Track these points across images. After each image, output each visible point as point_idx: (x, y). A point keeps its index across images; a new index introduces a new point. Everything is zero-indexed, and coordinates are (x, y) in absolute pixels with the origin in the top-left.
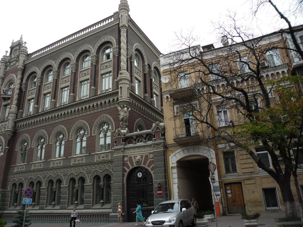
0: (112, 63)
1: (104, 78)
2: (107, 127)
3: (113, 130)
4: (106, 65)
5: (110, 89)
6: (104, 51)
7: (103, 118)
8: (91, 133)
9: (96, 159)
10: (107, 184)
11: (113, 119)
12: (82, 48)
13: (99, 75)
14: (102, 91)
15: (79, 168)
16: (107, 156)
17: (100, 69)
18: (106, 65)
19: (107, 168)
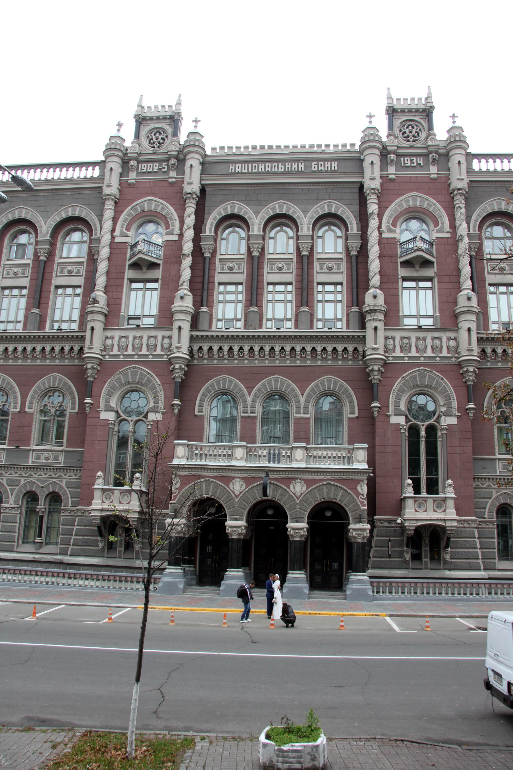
0: (85, 268)
1: (60, 295)
2: (61, 399)
3: (74, 409)
4: (70, 268)
5: (75, 321)
6: (68, 234)
7: (54, 382)
8: (23, 405)
9: (31, 460)
10: (50, 509)
11: (75, 386)
12: (17, 211)
13: (53, 288)
14: (53, 322)
16: (56, 458)
17: (55, 273)
18: (70, 268)
19: (55, 480)
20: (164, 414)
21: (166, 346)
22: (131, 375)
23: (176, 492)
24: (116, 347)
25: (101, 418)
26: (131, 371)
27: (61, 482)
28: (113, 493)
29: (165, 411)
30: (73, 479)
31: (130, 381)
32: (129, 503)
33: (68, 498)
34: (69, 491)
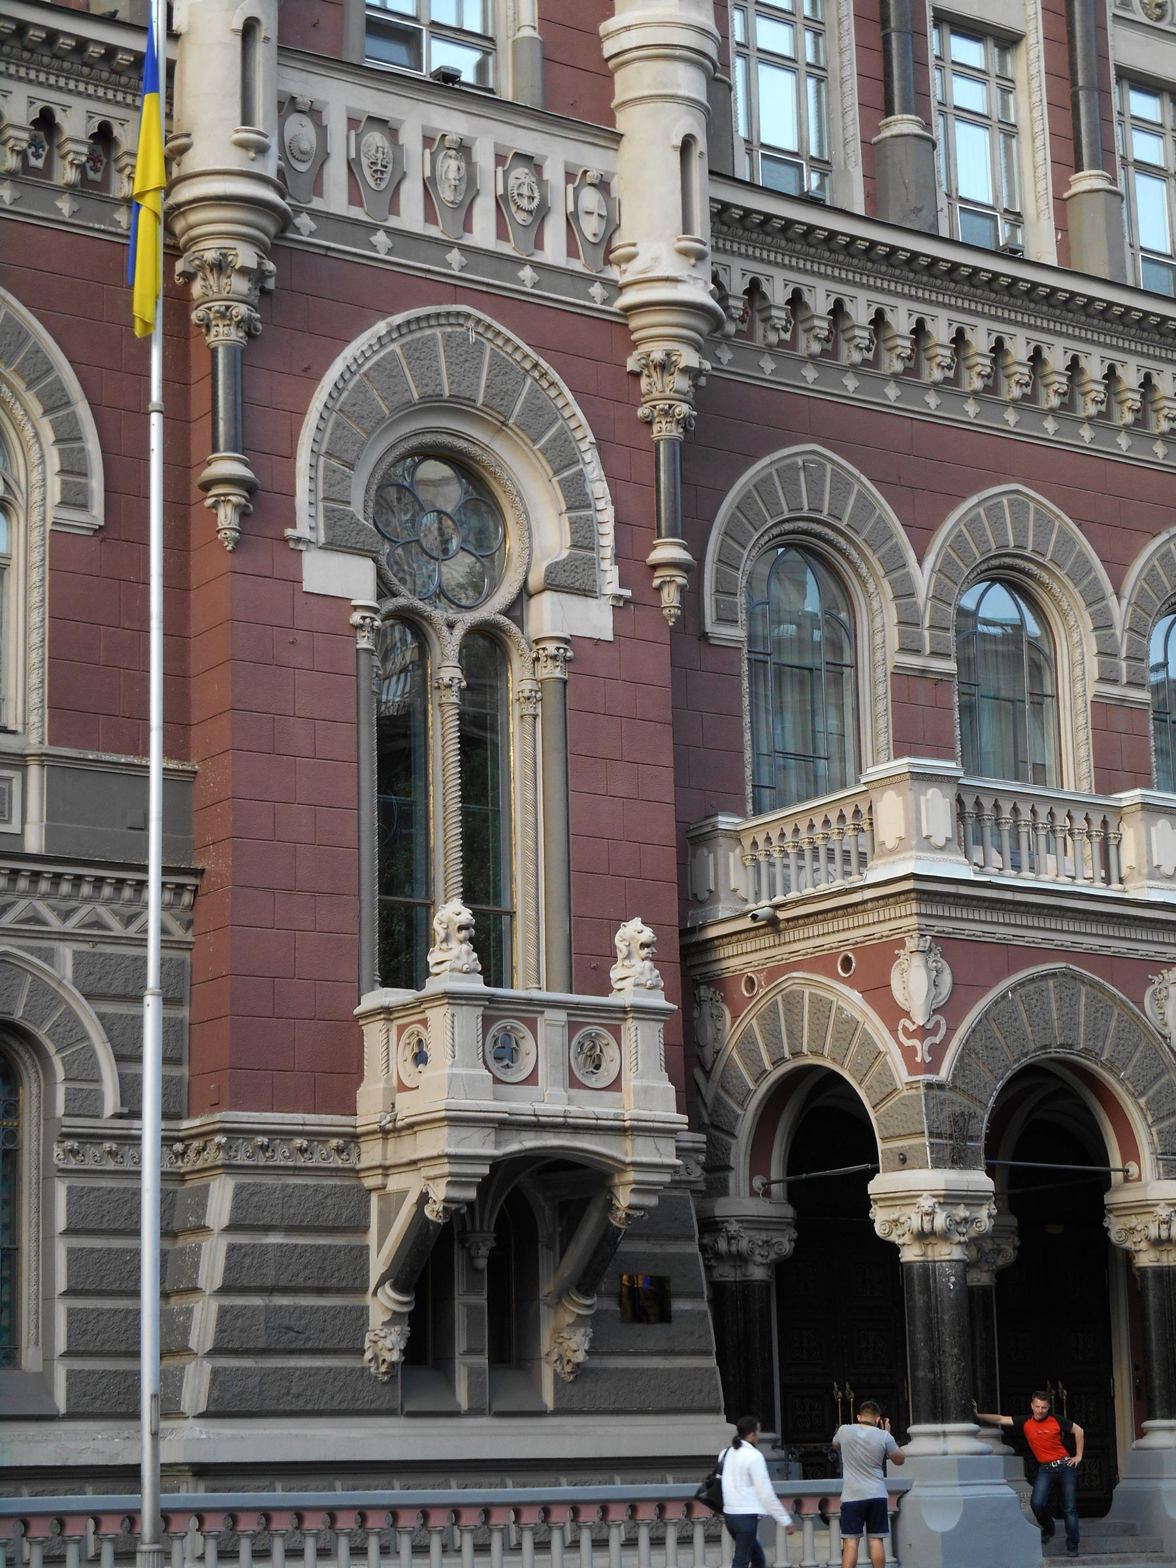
3: (84, 506)
15: (84, 912)
20: (621, 607)
21: (590, 227)
22: (450, 364)
23: (938, 1024)
24: (336, 173)
25: (307, 587)
26: (448, 337)
27: (48, 956)
28: (532, 1026)
29: (627, 593)
30: (116, 940)
31: (447, 393)
32: (616, 1085)
33: (96, 1065)
34: (101, 1017)
